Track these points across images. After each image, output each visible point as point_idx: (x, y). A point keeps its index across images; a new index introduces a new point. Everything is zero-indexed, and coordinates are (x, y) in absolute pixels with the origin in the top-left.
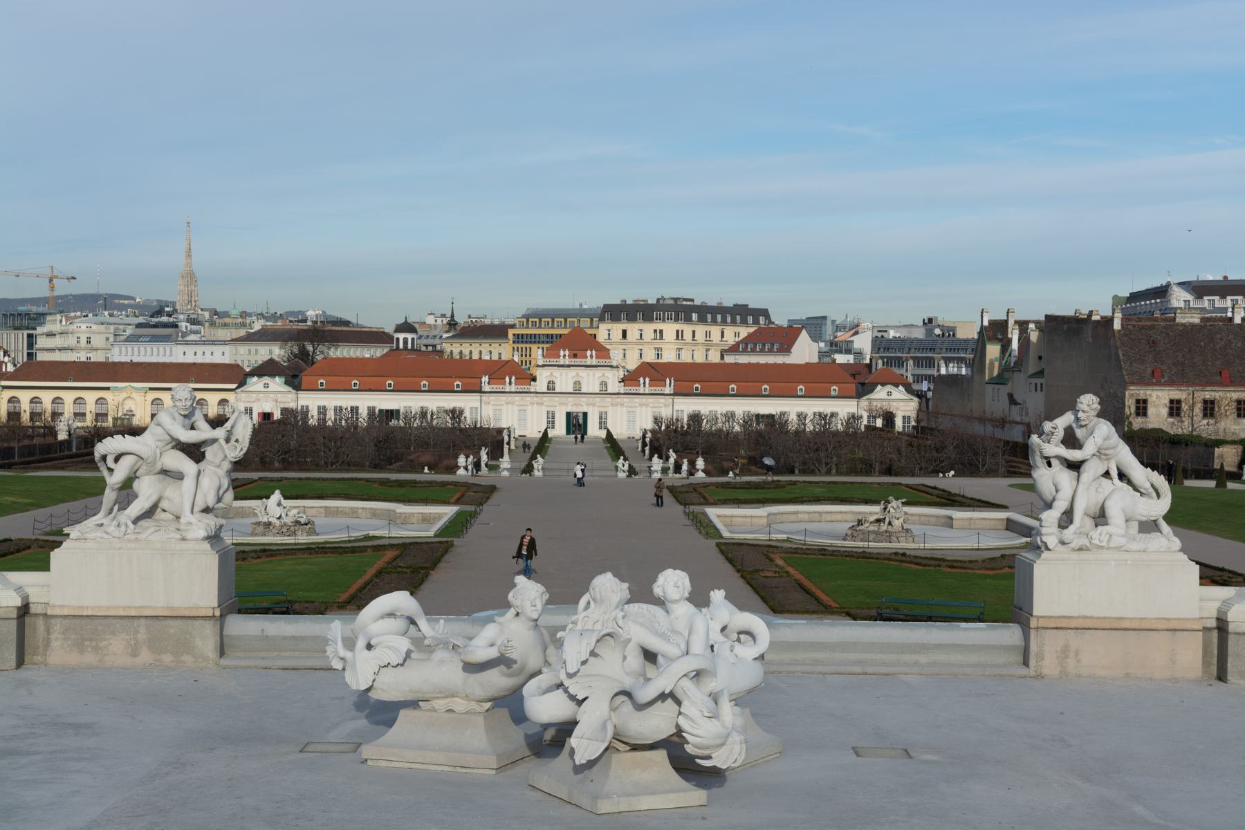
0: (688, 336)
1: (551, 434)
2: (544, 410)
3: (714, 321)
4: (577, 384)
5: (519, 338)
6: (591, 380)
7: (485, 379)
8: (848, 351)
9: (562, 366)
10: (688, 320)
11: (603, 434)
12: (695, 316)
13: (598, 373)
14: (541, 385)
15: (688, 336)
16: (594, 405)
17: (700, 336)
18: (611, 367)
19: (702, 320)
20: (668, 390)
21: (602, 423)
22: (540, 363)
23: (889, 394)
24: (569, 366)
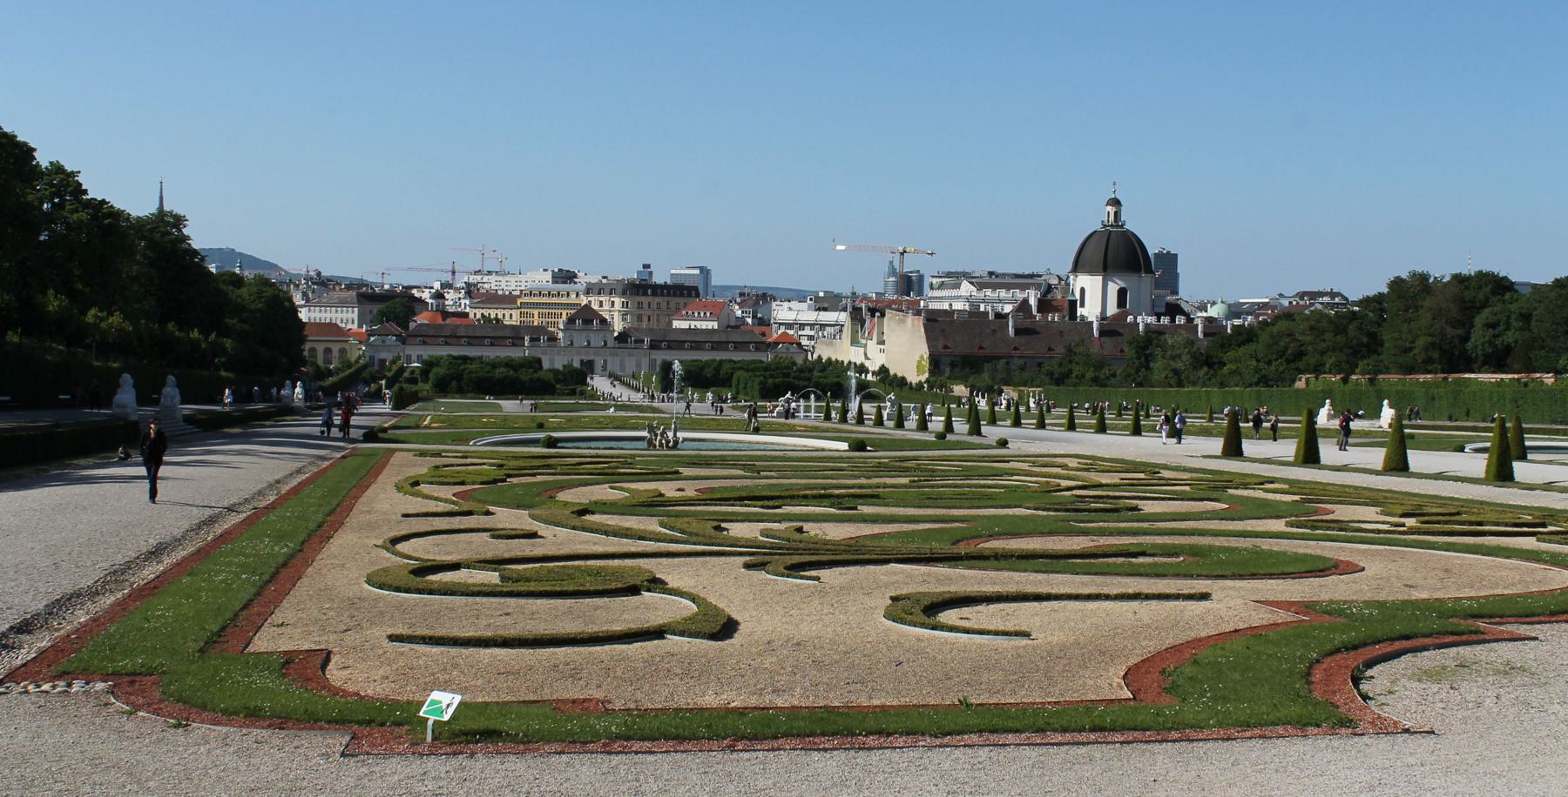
0: (645, 305)
6: (597, 341)
10: (645, 294)
15: (645, 305)
19: (654, 294)
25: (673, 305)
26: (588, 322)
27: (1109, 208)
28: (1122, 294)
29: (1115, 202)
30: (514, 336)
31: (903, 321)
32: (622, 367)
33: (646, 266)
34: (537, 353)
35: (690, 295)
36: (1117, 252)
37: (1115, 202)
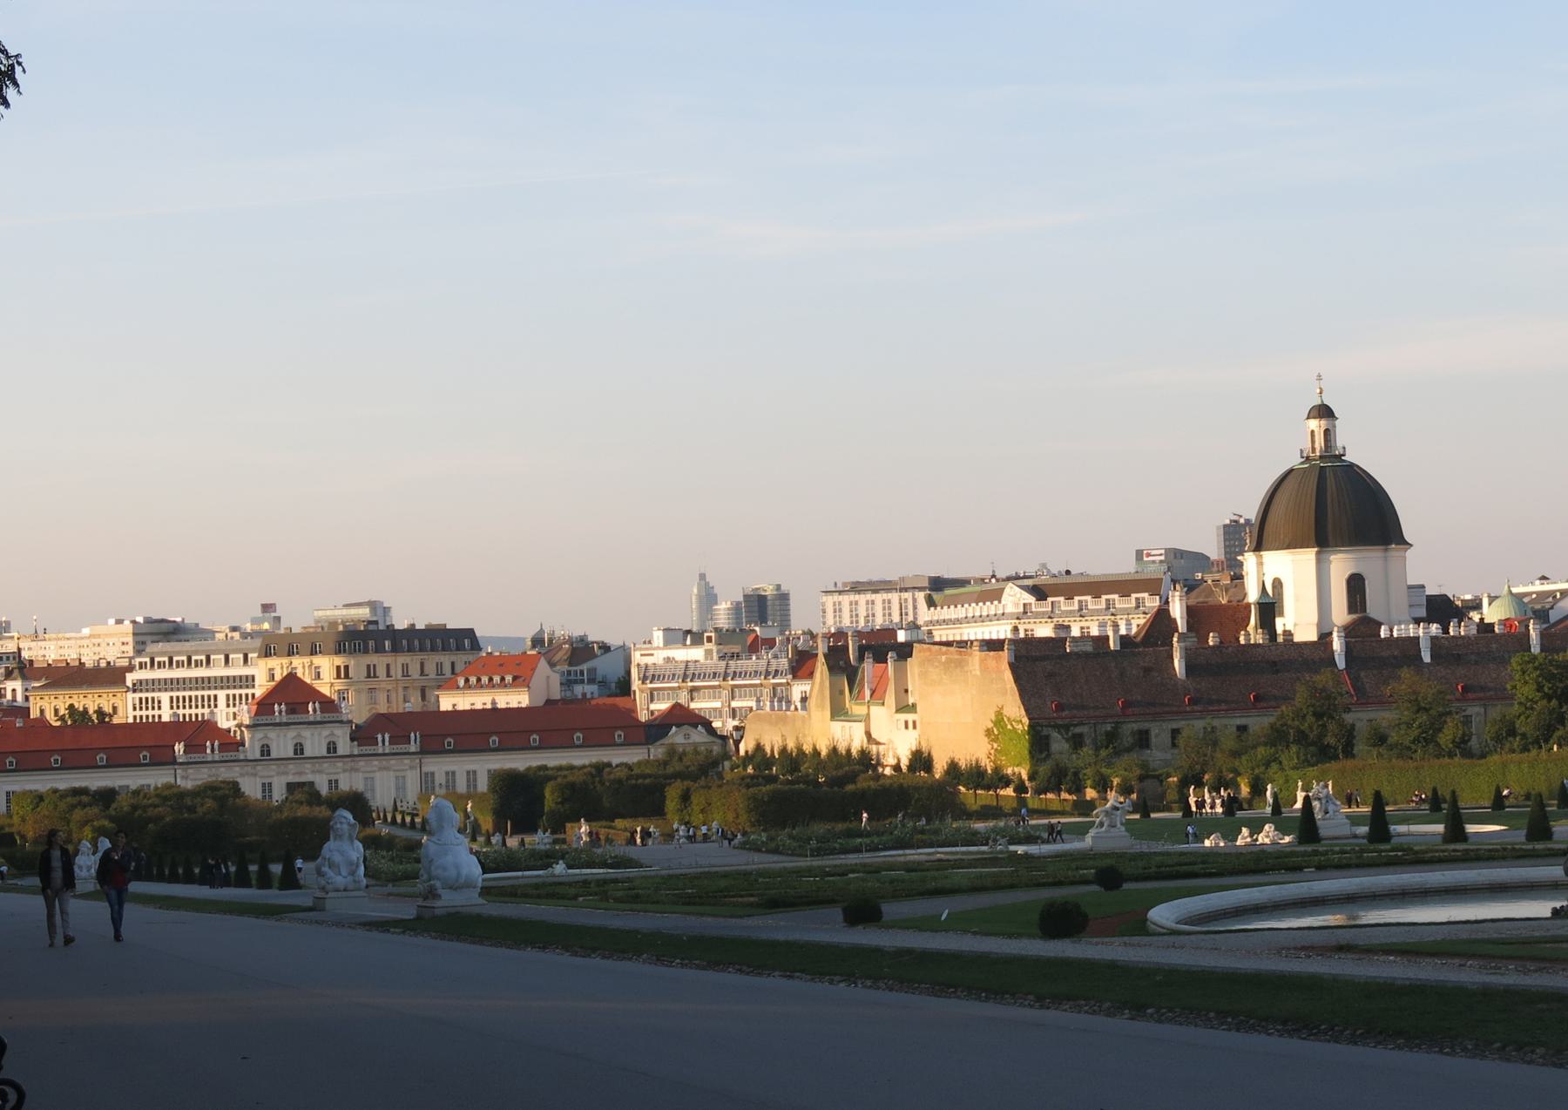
0: (381, 672)
2: (259, 782)
3: (410, 650)
4: (299, 749)
5: (137, 687)
6: (315, 743)
7: (179, 748)
8: (591, 681)
10: (379, 650)
13: (326, 733)
15: (381, 672)
16: (320, 772)
17: (397, 672)
18: (341, 722)
19: (396, 649)
20: (413, 748)
23: (687, 736)
24: (287, 724)
25: (431, 669)
26: (296, 708)
27: (1314, 424)
28: (1356, 585)
29: (1324, 412)
30: (150, 743)
31: (960, 664)
33: (267, 608)
34: (225, 773)
35: (460, 648)
36: (1340, 505)
37: (1324, 412)
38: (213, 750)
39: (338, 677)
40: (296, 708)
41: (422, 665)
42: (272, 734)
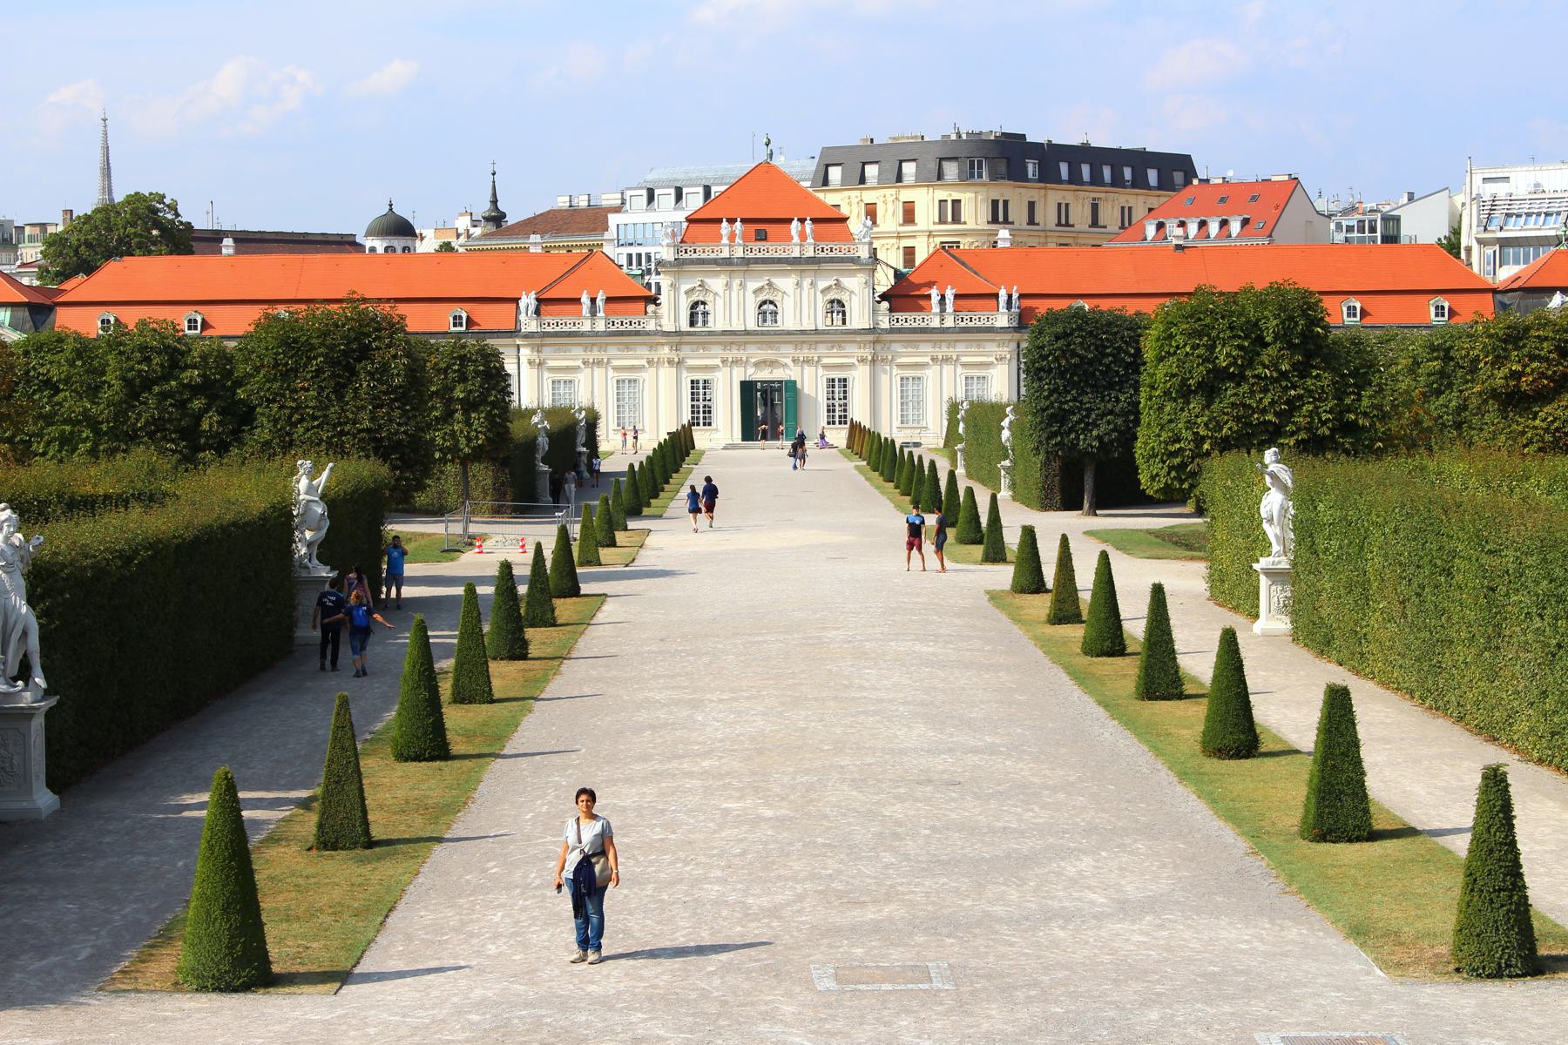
1: (701, 438)
2: (687, 378)
3: (1075, 179)
4: (767, 309)
6: (800, 303)
9: (727, 262)
10: (1016, 174)
11: (839, 436)
12: (1031, 168)
14: (671, 313)
15: (1018, 213)
18: (855, 260)
19: (1048, 176)
20: (1002, 320)
21: (837, 413)
22: (668, 254)
26: (762, 226)
32: (910, 403)
35: (1165, 184)
38: (593, 312)
39: (942, 221)
40: (762, 226)
41: (1095, 208)
42: (717, 283)
